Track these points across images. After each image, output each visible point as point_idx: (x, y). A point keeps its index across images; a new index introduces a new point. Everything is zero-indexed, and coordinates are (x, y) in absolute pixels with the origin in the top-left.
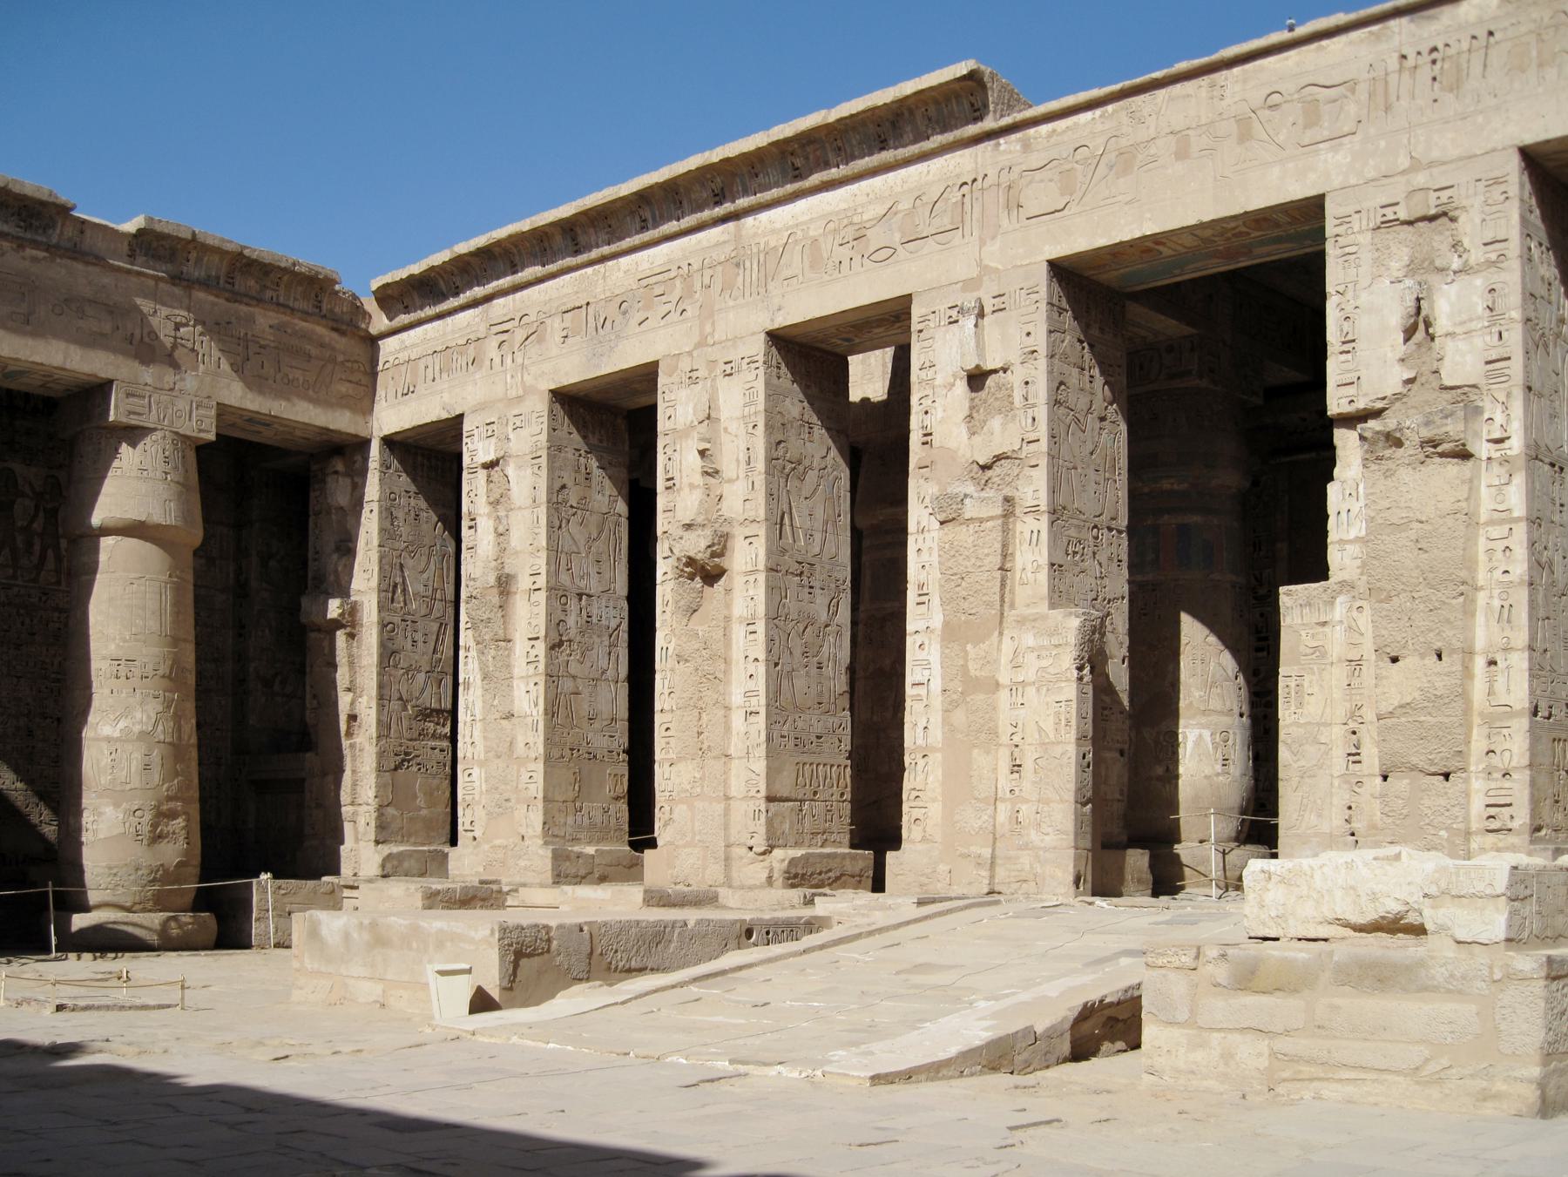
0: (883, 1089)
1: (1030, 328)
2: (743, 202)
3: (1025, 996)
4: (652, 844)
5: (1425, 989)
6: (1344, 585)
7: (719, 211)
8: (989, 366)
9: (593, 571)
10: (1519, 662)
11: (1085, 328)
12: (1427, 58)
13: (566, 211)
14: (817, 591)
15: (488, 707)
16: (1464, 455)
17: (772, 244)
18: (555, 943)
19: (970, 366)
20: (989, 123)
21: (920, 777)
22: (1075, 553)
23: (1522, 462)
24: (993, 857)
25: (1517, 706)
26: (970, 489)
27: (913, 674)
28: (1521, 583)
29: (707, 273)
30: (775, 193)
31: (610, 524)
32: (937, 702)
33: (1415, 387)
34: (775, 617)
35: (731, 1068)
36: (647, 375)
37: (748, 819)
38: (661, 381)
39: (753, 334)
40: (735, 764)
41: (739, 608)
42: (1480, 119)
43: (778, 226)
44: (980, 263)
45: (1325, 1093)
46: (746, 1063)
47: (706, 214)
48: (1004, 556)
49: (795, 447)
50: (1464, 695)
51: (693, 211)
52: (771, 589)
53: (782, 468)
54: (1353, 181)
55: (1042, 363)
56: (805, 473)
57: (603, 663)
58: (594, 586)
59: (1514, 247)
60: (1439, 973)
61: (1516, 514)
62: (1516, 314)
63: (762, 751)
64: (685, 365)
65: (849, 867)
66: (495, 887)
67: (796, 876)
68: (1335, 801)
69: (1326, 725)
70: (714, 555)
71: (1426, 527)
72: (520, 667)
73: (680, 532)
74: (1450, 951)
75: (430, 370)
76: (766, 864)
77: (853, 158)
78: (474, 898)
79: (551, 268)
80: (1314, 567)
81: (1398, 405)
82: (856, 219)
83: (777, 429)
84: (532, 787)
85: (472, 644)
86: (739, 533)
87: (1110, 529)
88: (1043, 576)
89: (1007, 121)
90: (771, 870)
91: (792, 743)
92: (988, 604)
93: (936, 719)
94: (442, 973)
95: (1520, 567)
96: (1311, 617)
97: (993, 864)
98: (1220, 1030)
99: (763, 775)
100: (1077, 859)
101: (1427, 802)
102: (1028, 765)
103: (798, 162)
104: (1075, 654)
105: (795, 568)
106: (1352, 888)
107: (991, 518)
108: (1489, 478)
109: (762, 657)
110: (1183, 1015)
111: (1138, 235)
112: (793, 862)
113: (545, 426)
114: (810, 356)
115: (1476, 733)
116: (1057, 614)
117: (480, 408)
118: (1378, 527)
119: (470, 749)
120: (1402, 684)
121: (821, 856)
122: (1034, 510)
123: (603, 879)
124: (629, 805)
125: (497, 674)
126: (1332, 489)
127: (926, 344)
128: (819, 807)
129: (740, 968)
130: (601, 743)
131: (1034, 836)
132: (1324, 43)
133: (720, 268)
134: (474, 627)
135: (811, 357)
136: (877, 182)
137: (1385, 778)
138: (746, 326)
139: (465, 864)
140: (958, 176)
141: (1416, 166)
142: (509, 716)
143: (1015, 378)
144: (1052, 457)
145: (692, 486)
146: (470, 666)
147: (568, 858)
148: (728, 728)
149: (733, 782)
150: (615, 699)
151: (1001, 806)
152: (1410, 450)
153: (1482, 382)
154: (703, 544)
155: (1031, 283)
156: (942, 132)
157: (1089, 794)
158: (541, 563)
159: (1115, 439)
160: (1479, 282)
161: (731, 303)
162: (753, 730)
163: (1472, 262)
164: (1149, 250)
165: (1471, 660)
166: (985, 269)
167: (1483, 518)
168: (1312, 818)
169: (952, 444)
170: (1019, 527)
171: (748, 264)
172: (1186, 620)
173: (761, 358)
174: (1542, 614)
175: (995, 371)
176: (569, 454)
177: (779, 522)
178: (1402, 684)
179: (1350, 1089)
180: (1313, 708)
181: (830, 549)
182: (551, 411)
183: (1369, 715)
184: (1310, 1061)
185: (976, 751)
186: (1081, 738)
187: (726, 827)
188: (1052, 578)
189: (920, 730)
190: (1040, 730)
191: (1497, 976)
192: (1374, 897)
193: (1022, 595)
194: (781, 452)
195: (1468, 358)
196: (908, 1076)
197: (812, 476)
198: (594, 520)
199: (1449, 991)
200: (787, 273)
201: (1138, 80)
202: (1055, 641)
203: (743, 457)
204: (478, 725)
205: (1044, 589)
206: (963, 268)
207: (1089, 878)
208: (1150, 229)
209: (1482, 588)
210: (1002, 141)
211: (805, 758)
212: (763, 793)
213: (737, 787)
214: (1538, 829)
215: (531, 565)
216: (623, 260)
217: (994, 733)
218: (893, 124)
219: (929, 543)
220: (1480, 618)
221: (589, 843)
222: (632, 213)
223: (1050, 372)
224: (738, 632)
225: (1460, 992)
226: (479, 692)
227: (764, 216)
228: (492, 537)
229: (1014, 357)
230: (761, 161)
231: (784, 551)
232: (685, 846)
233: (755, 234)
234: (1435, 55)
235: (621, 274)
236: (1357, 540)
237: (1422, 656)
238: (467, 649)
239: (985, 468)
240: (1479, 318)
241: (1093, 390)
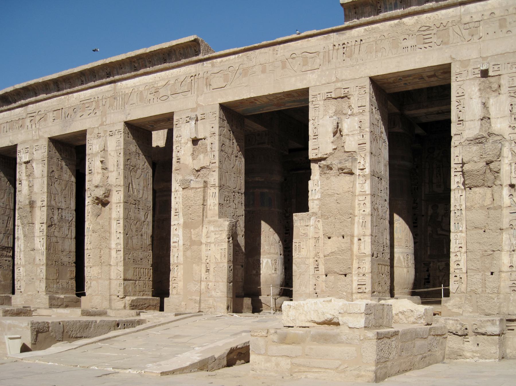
0: (165, 377)
1: (213, 125)
2: (117, 77)
3: (211, 346)
4: (84, 294)
5: (339, 342)
6: (314, 214)
7: (108, 80)
8: (199, 137)
9: (63, 200)
10: (368, 239)
11: (231, 126)
12: (342, 47)
13: (55, 76)
14: (141, 210)
15: (26, 247)
16: (351, 173)
17: (127, 92)
18: (50, 329)
19: (193, 137)
20: (201, 57)
21: (176, 273)
22: (227, 200)
23: (369, 176)
24: (200, 300)
25: (367, 254)
26: (193, 178)
27: (173, 239)
28: (369, 214)
29: (104, 100)
30: (128, 75)
31: (69, 185)
32: (181, 248)
33: (336, 151)
34: (126, 218)
35: (113, 370)
36: (83, 134)
37: (117, 286)
38: (88, 136)
39: (120, 122)
40: (113, 268)
41: (114, 215)
42: (358, 67)
43: (129, 86)
44: (197, 103)
45: (309, 376)
46: (118, 369)
47: (104, 81)
48: (204, 200)
49: (134, 161)
50: (351, 250)
51: (99, 79)
52: (125, 209)
53: (129, 168)
54: (318, 84)
55: (217, 137)
56: (137, 170)
57: (67, 232)
58: (63, 206)
59: (367, 108)
60: (344, 338)
61: (367, 193)
62: (368, 130)
63: (122, 264)
64: (96, 131)
65: (152, 303)
66: (28, 309)
67: (134, 306)
68: (311, 283)
69: (308, 258)
70: (105, 197)
71: (340, 196)
72: (37, 233)
73: (94, 188)
74: (347, 331)
75: (5, 128)
76: (124, 301)
77: (155, 65)
78: (21, 312)
79: (49, 95)
80: (305, 208)
81: (331, 156)
82: (155, 86)
83: (127, 155)
84: (42, 274)
85: (20, 224)
86: (114, 190)
87: (239, 193)
88: (217, 208)
89: (206, 56)
90: (125, 304)
91: (132, 260)
92: (199, 216)
93: (181, 254)
94: (11, 339)
95: (368, 210)
96: (303, 223)
97: (200, 302)
98: (275, 356)
99: (122, 271)
100: (228, 301)
101: (340, 283)
102: (212, 270)
103: (136, 65)
104: (227, 233)
105: (133, 202)
106: (317, 310)
107: (199, 188)
108: (359, 181)
109: (122, 232)
110: (263, 352)
111: (249, 97)
112: (133, 301)
113: (47, 150)
114: (139, 131)
116: (221, 220)
117: (24, 142)
118: (325, 195)
119: (19, 261)
120: (331, 246)
121: (142, 299)
122: (214, 186)
123: (67, 306)
124: (76, 281)
125: (29, 235)
126: (310, 182)
127: (178, 129)
128: (141, 283)
129: (115, 337)
130: (66, 259)
131: (213, 293)
132: (310, 39)
133: (108, 99)
134: (21, 219)
135: (139, 131)
136: (163, 73)
137: (326, 276)
138: (117, 120)
139: (18, 301)
140: (190, 73)
141: (338, 80)
142: (33, 250)
143: (208, 142)
144: (220, 168)
145: (98, 173)
146: (19, 232)
147: (54, 299)
148: (110, 256)
149: (112, 274)
150: (71, 245)
151: (203, 283)
152: (335, 171)
153: (357, 151)
154: (102, 193)
155: (214, 111)
156: (185, 58)
157: (232, 280)
158: (45, 197)
159: (240, 163)
160: (356, 119)
161: (112, 111)
162: (119, 256)
163: (354, 112)
164: (252, 102)
165: (353, 238)
166: (199, 105)
168: (303, 288)
169: (187, 163)
170: (209, 191)
171: (118, 98)
172: (263, 223)
173: (122, 130)
174: (375, 224)
175: (201, 139)
176: (55, 160)
177: (128, 186)
178: (331, 246)
179: (316, 374)
180: (304, 253)
181: (145, 196)
182: (49, 145)
183: (321, 255)
184: (304, 366)
185: (194, 265)
186: (229, 261)
187: (110, 289)
188: (219, 208)
189: (175, 258)
190: (216, 258)
191: (362, 338)
192: (323, 314)
193: (209, 213)
194: (129, 163)
195: (353, 143)
196: (173, 372)
197: (139, 171)
198: (64, 183)
199: (347, 343)
200: (131, 102)
201: (250, 46)
202: (220, 229)
203: (116, 164)
204: (22, 253)
205: (217, 212)
206: (191, 104)
207: (232, 307)
208: (253, 95)
209: (357, 216)
210: (205, 63)
211: (136, 266)
212: (122, 278)
213: (113, 275)
214: (374, 292)
215: (41, 198)
216: (75, 95)
217: (200, 259)
218: (169, 54)
219: (179, 195)
220: (356, 225)
221: (62, 294)
222: (78, 78)
223: (220, 140)
224: (114, 223)
225: (350, 344)
226: (23, 241)
227: (124, 83)
228: (27, 187)
229: (208, 135)
230: (123, 64)
231: (129, 196)
232: (95, 295)
233: (121, 88)
234: (344, 46)
235: (74, 99)
236: (318, 199)
237: (338, 237)
238: (18, 226)
239: (198, 171)
240: (357, 130)
241: (234, 147)
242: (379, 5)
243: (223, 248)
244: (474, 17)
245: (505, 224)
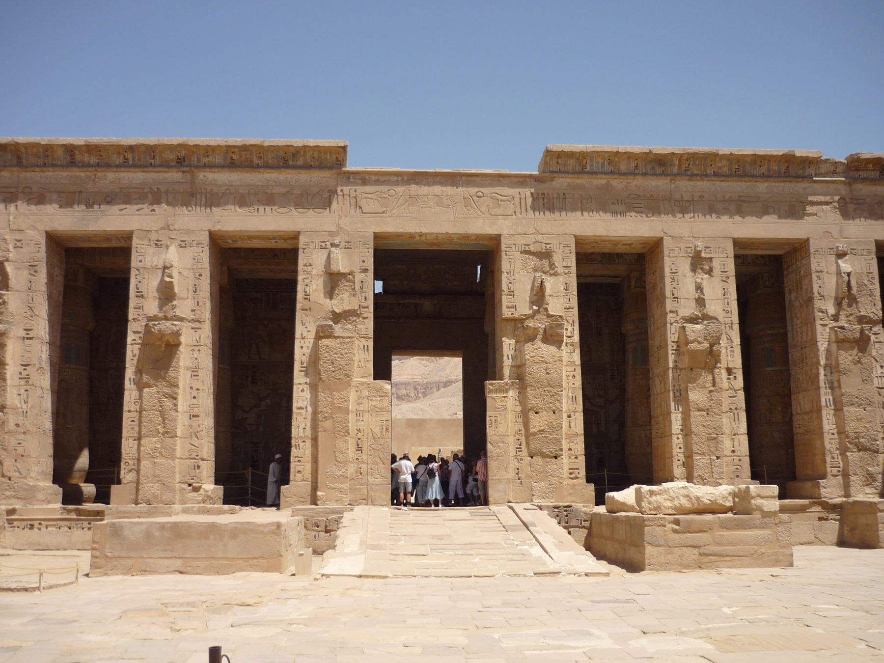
4: (119, 482)
17: (215, 190)
38: (135, 241)
64: (154, 237)
115: (564, 442)
141: (537, 232)
166: (340, 228)
167: (564, 363)
171: (199, 196)
180: (502, 429)
189: (301, 430)
203: (191, 288)
219: (307, 344)
220: (564, 401)
229: (356, 270)
235: (107, 182)
242: (585, 161)
243: (384, 419)
244: (684, 196)
245: (725, 408)
